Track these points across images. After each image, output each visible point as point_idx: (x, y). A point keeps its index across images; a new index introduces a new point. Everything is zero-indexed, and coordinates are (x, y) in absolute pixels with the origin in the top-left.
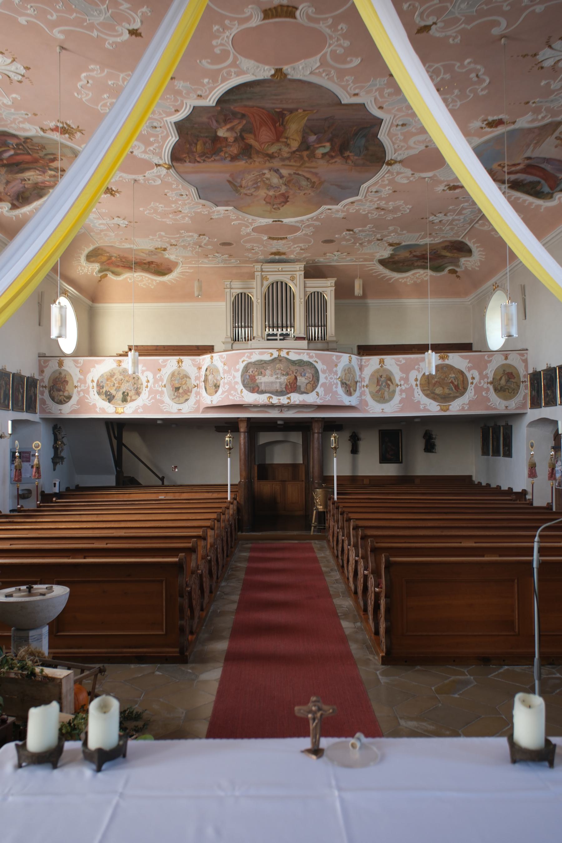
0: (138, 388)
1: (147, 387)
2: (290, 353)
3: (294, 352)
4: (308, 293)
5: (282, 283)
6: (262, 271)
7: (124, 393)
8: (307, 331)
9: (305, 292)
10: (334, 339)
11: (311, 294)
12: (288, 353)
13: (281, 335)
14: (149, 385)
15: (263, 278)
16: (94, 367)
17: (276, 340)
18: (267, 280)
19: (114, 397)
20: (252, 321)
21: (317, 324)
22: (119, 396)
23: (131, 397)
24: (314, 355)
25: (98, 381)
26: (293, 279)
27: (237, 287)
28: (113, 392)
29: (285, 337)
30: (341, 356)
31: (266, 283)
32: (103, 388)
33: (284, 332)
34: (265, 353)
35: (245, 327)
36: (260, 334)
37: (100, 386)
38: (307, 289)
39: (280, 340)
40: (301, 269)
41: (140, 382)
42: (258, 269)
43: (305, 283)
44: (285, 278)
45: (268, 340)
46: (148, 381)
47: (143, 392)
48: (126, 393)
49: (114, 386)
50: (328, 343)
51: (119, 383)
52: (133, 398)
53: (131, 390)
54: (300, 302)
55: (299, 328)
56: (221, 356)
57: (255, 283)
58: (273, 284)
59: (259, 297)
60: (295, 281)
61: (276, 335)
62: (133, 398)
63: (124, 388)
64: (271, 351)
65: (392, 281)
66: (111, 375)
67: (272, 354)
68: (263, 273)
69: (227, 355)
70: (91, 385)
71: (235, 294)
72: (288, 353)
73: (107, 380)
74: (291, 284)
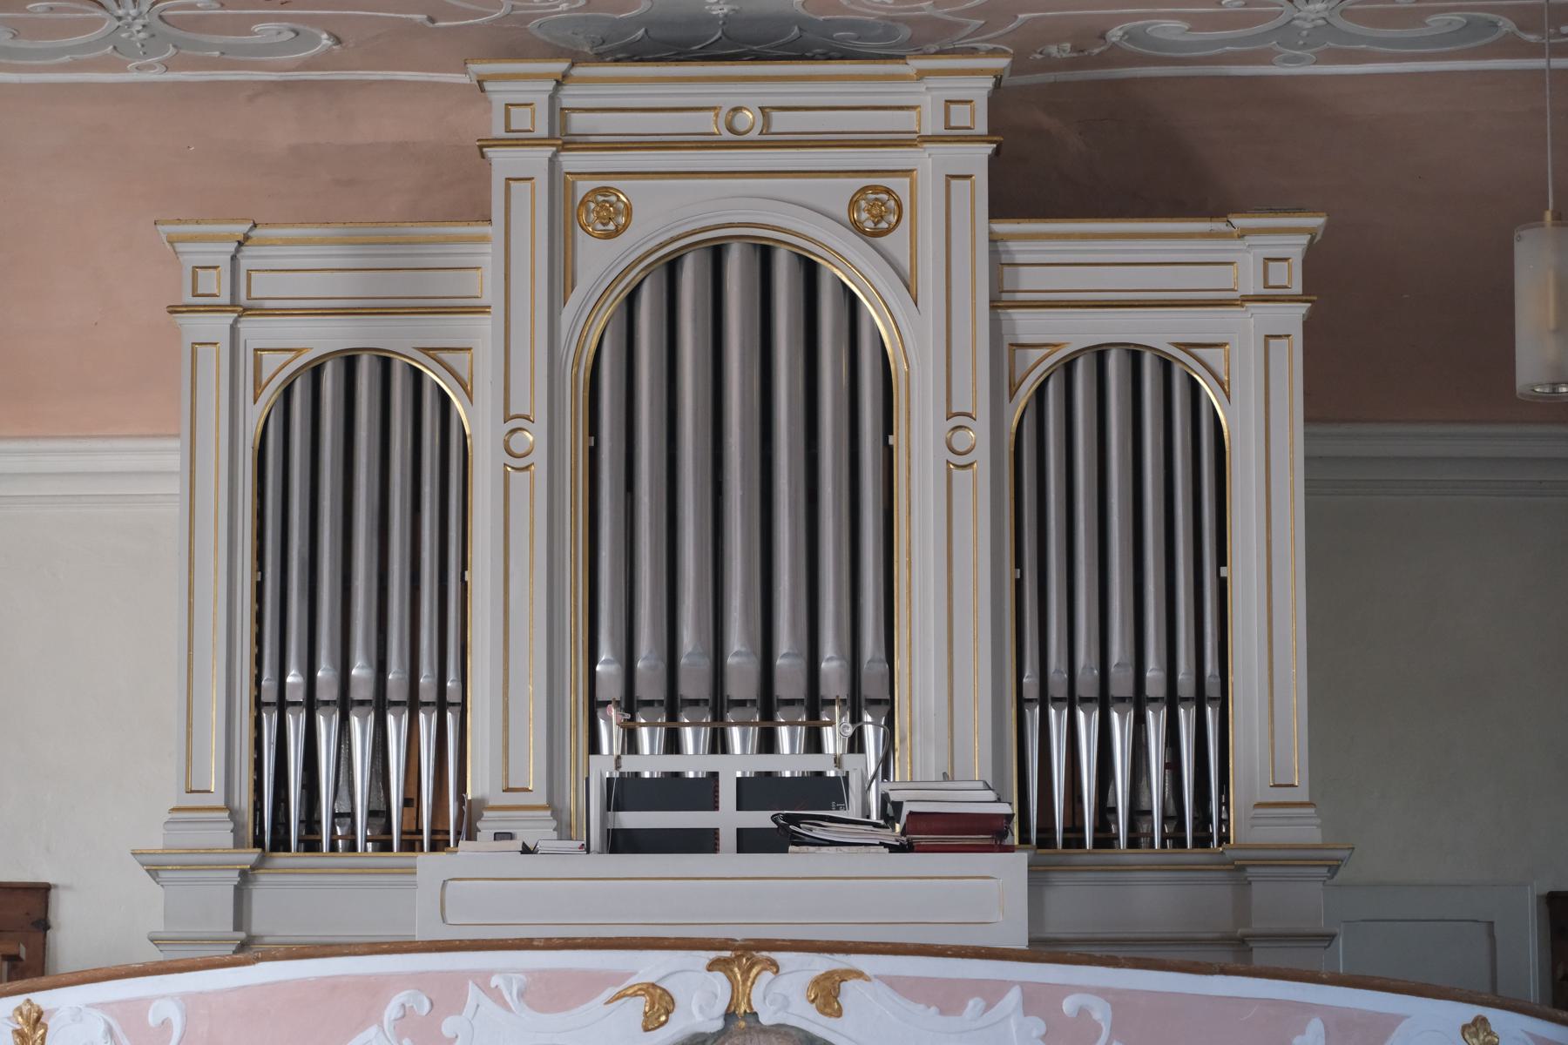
2: (851, 992)
3: (893, 983)
4: (1035, 367)
5: (765, 254)
6: (563, 140)
8: (1023, 757)
9: (1004, 350)
10: (1306, 831)
11: (1068, 366)
12: (827, 994)
13: (753, 791)
17: (704, 842)
20: (452, 646)
21: (1121, 682)
24: (1101, 1012)
26: (875, 216)
27: (307, 296)
29: (794, 813)
30: (1389, 1023)
31: (601, 261)
33: (790, 759)
34: (589, 984)
35: (380, 705)
36: (532, 773)
38: (1026, 325)
39: (749, 841)
40: (960, 116)
42: (521, 119)
43: (998, 265)
44: (802, 210)
45: (620, 842)
50: (1237, 869)
54: (956, 460)
55: (945, 723)
56: (131, 1012)
57: (488, 258)
58: (672, 267)
59: (531, 396)
60: (896, 243)
61: (703, 793)
64: (650, 966)
67: (660, 1005)
68: (572, 161)
69: (190, 1002)
72: (827, 994)
74: (851, 264)
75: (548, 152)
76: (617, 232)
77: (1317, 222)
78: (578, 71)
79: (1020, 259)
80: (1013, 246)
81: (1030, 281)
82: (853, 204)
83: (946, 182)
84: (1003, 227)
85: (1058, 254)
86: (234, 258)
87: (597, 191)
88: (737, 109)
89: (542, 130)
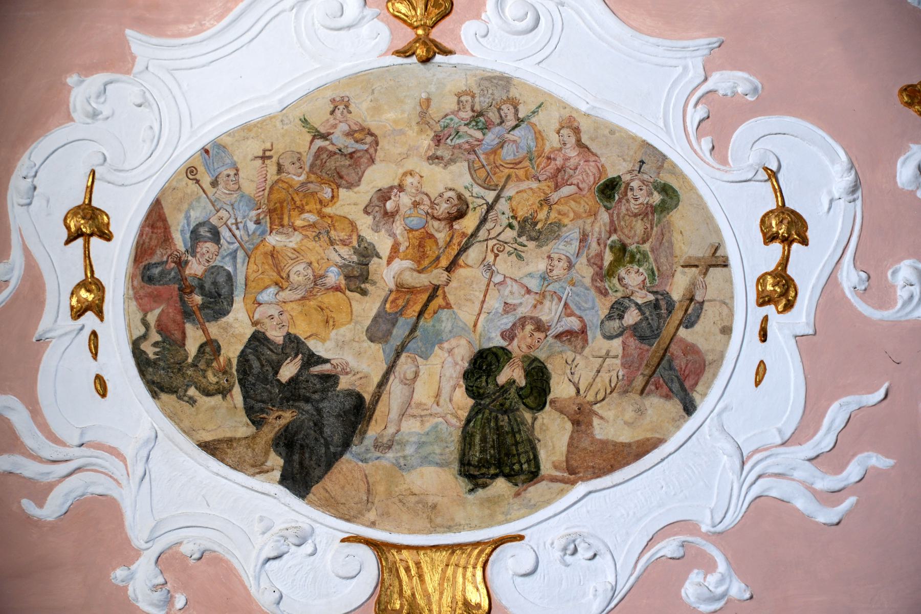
0: (660, 306)
1: (780, 290)
7: (484, 364)
14: (807, 267)
16: (119, 61)
19: (358, 411)
22: (429, 399)
23: (580, 418)
25: (156, 220)
28: (349, 353)
32: (217, 300)
37: (177, 284)
41: (687, 242)
46: (786, 228)
47: (741, 352)
48: (512, 374)
49: (358, 277)
51: (421, 248)
52: (613, 425)
53: (576, 337)
62: (613, 425)
63: (485, 303)
66: (328, 154)
70: (63, 267)
73: (277, 210)
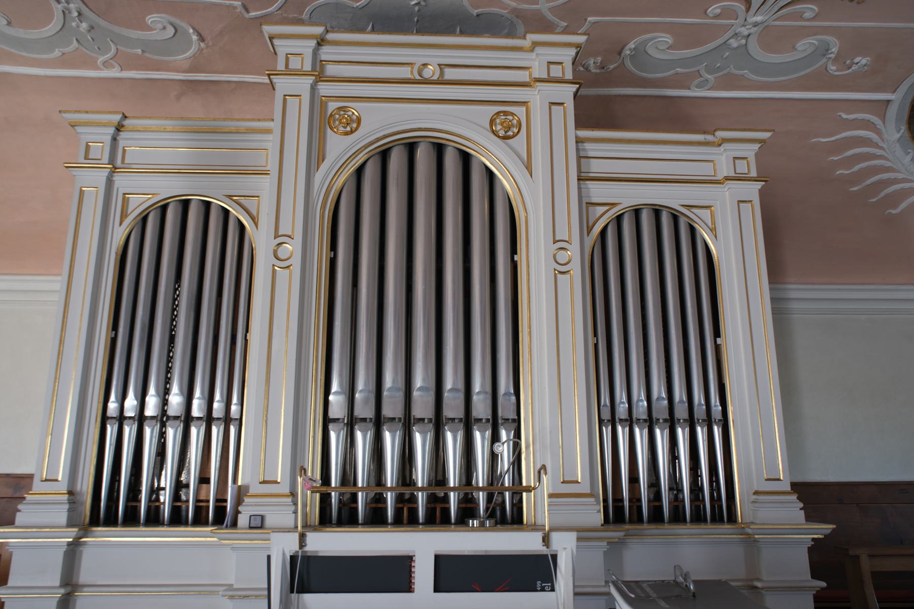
5: (439, 149)
6: (319, 74)
9: (586, 205)
11: (619, 219)
15: (323, 120)
18: (352, 125)
27: (160, 163)
31: (339, 147)
38: (598, 192)
40: (556, 72)
42: (295, 63)
57: (271, 142)
58: (384, 155)
59: (292, 222)
60: (519, 142)
65: (904, 205)
68: (325, 89)
71: (138, 203)
74: (491, 154)
75: (310, 80)
76: (352, 132)
77: (766, 135)
78: (330, 36)
79: (591, 154)
80: (588, 146)
81: (596, 167)
82: (492, 122)
83: (548, 108)
84: (583, 133)
85: (613, 151)
86: (114, 139)
87: (340, 108)
88: (425, 65)
89: (308, 67)
